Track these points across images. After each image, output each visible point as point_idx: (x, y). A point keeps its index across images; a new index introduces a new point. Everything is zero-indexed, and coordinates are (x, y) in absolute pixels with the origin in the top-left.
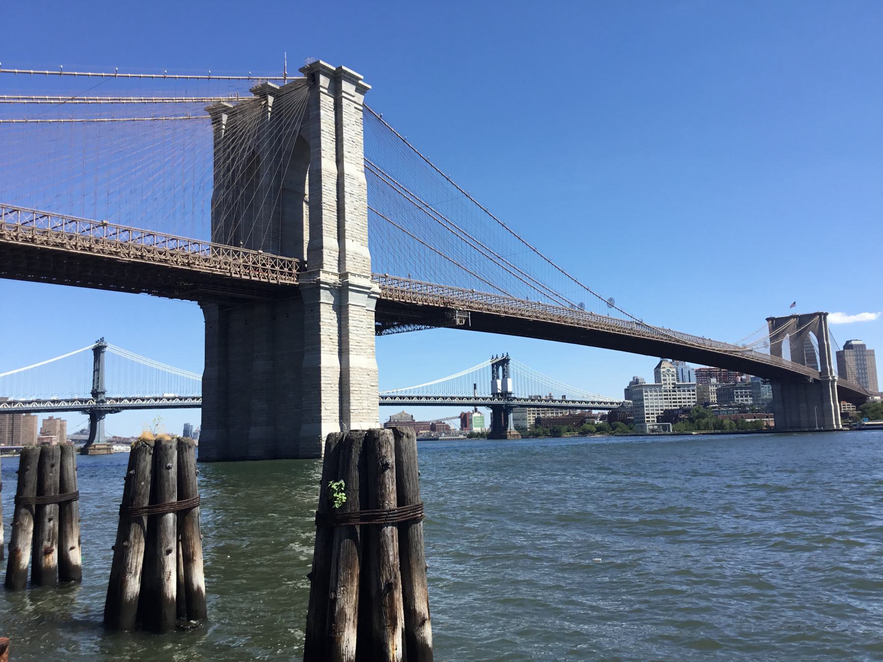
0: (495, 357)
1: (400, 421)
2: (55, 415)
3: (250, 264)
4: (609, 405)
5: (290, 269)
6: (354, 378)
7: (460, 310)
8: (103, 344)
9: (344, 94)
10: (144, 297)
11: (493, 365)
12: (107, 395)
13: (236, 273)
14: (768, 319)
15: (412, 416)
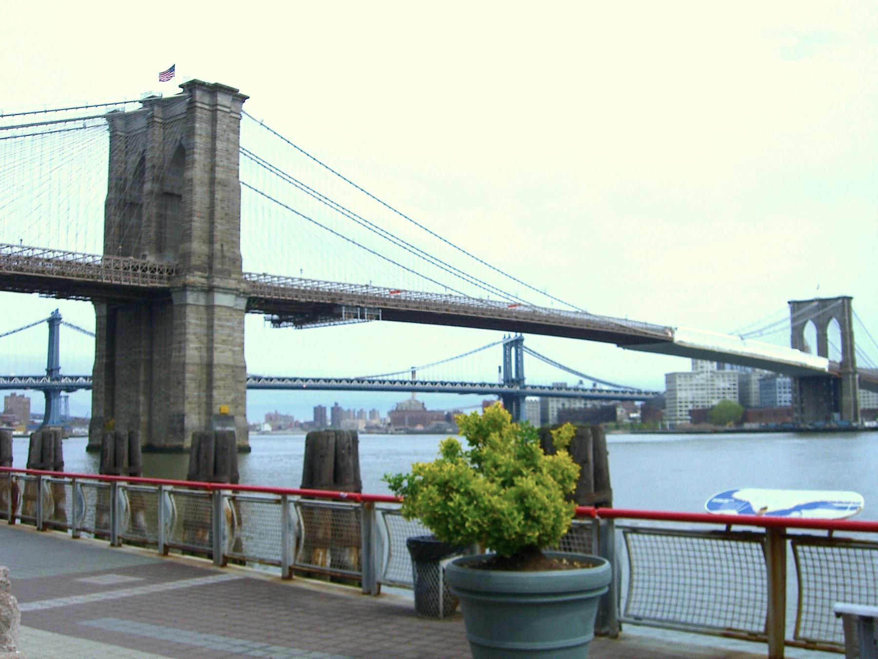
0: (507, 337)
1: (408, 409)
2: (19, 392)
3: (121, 270)
4: (643, 396)
5: (161, 273)
6: (218, 374)
7: (347, 307)
8: (58, 317)
9: (219, 107)
10: (36, 295)
11: (505, 346)
12: (61, 372)
13: (107, 279)
14: (789, 303)
15: (423, 404)
